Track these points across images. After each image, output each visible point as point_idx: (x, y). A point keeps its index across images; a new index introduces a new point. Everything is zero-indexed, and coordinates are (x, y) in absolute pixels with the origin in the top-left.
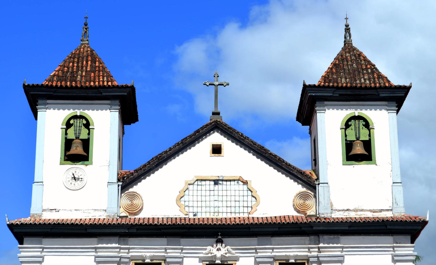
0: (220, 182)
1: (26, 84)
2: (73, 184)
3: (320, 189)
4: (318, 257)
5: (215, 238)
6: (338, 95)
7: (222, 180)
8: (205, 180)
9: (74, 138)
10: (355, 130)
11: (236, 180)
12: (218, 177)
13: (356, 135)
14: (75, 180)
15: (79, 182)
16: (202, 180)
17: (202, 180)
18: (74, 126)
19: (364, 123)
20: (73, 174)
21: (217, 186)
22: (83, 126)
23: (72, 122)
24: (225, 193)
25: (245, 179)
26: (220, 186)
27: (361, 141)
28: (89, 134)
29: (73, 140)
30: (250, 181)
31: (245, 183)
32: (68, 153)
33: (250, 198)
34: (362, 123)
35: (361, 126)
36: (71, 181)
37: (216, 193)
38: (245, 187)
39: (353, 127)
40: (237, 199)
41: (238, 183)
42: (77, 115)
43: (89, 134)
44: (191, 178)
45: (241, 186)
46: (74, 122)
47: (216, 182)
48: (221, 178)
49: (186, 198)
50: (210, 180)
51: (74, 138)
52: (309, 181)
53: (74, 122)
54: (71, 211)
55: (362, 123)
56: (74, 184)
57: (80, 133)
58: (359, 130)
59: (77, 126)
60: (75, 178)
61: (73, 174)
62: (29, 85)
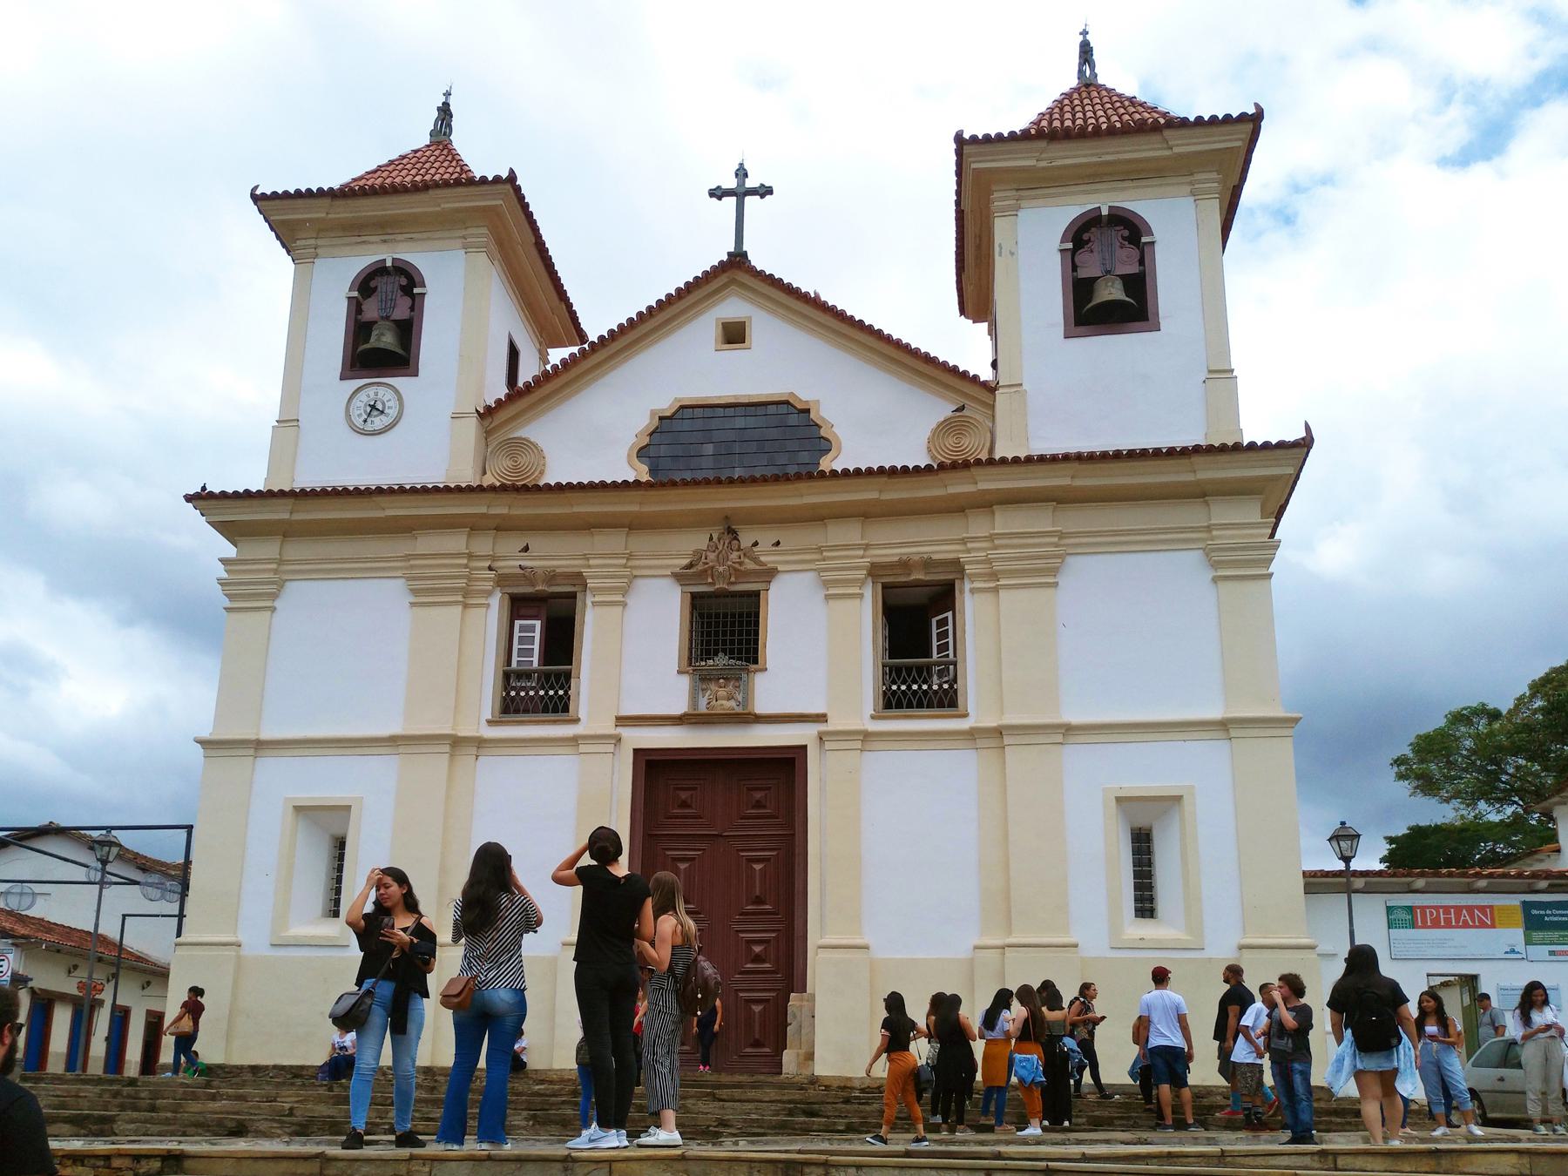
4: (988, 561)
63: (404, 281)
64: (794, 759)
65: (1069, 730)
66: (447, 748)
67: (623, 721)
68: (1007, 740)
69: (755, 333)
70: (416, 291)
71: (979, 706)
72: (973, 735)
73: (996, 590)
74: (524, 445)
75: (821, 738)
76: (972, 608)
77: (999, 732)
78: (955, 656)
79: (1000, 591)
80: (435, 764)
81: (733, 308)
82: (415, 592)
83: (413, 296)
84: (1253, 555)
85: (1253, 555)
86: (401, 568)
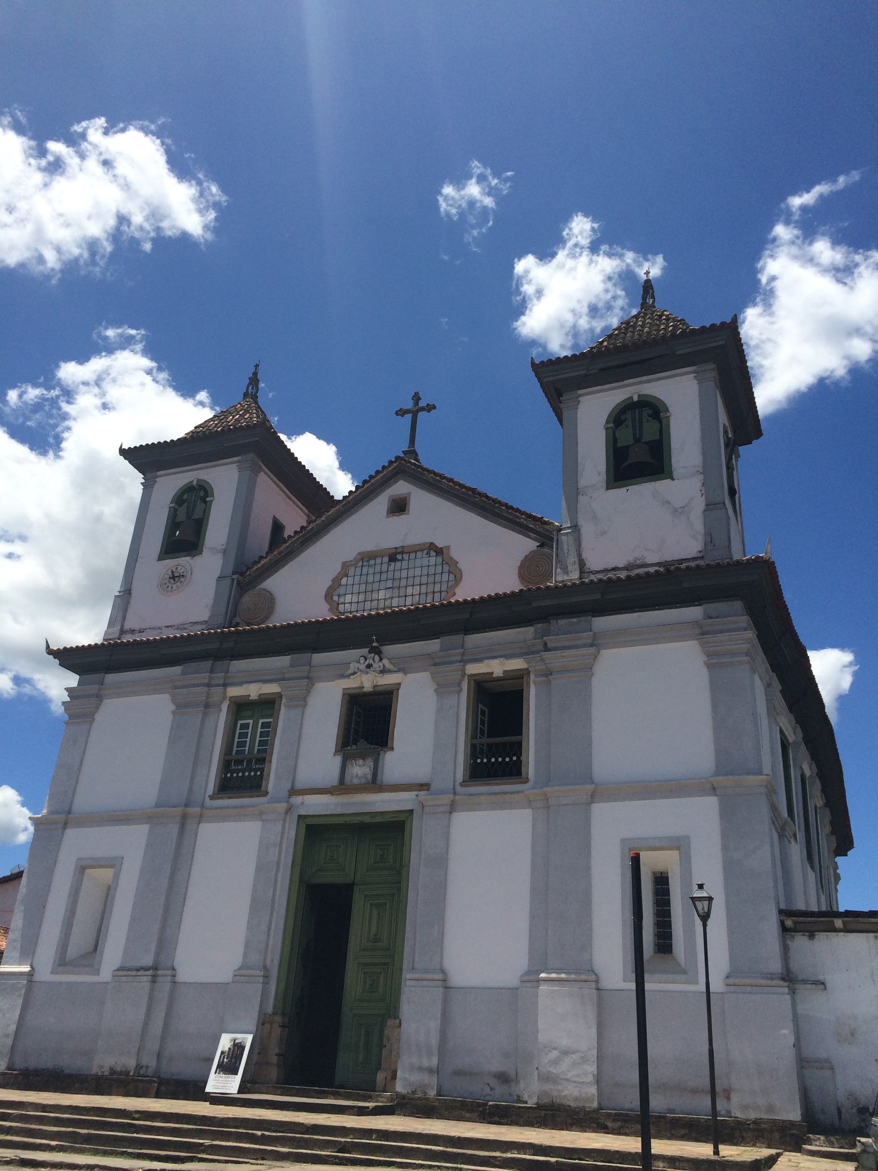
0: (399, 557)
2: (170, 588)
6: (596, 371)
7: (402, 553)
12: (396, 548)
13: (634, 435)
19: (650, 412)
21: (393, 564)
24: (404, 574)
25: (439, 545)
26: (398, 564)
27: (644, 443)
30: (448, 548)
31: (439, 552)
34: (647, 412)
37: (390, 575)
38: (439, 559)
40: (424, 580)
44: (350, 556)
47: (393, 556)
49: (342, 590)
52: (547, 530)
54: (160, 628)
55: (647, 412)
58: (641, 428)
61: (173, 572)
63: (202, 494)
69: (413, 504)
70: (208, 499)
81: (401, 487)
83: (205, 502)
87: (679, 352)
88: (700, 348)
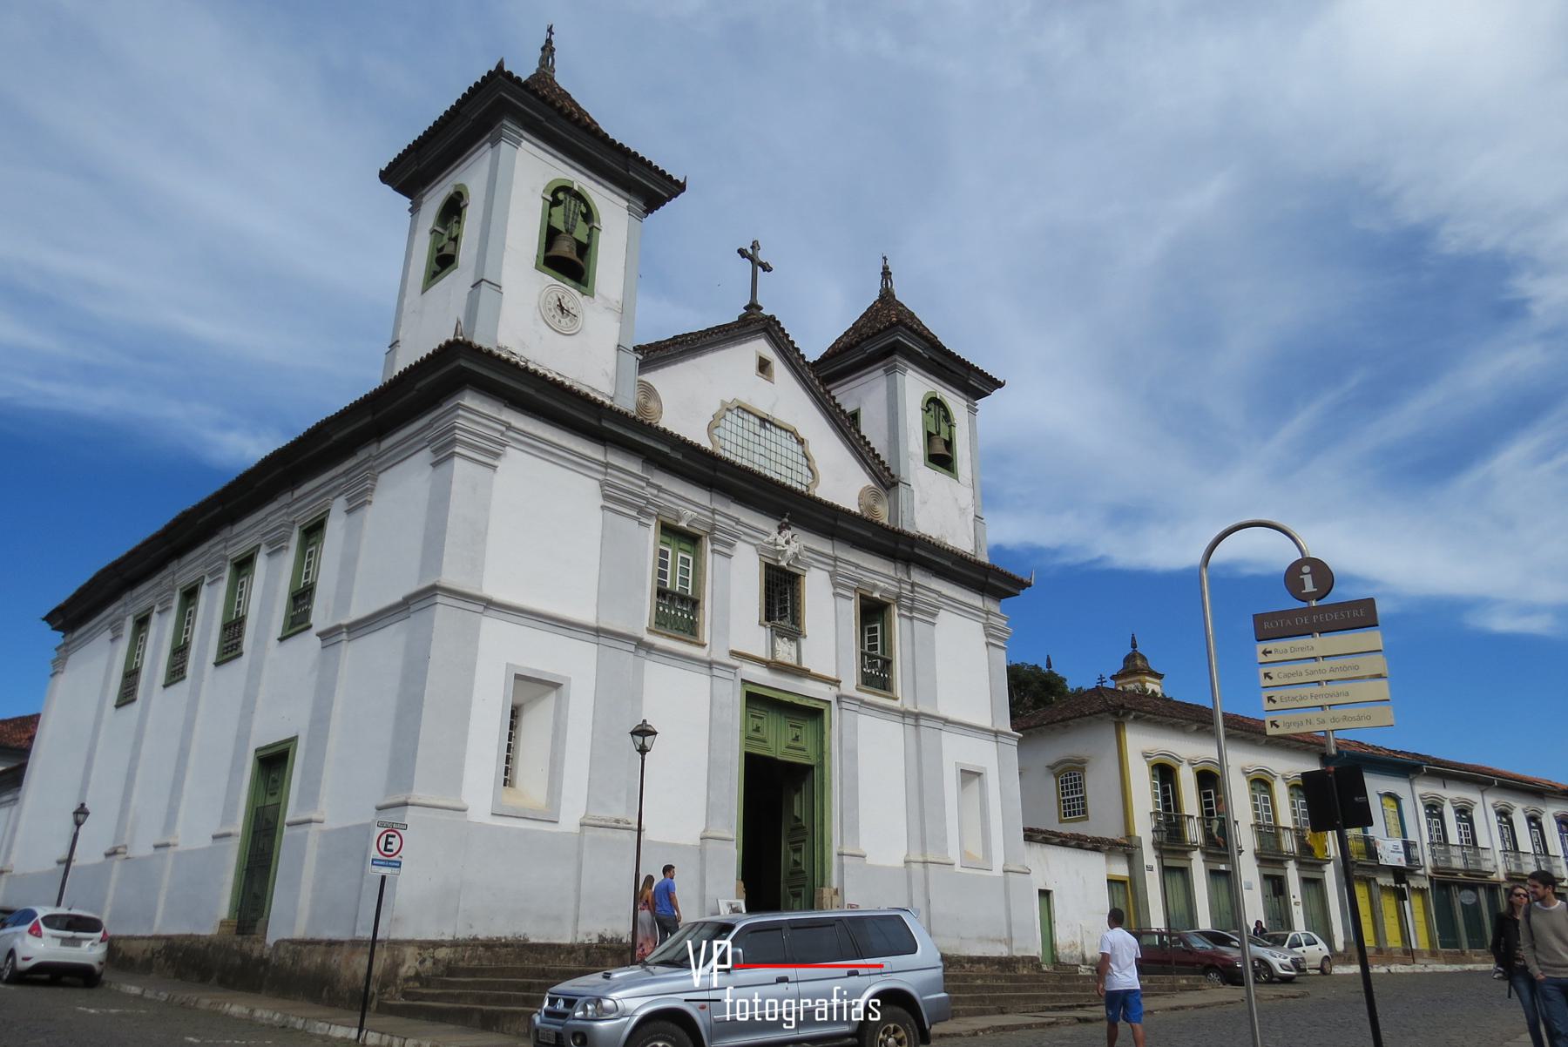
1: (506, 69)
3: (902, 488)
5: (777, 519)
8: (749, 412)
9: (564, 231)
10: (935, 419)
11: (790, 432)
14: (563, 313)
15: (567, 320)
16: (744, 410)
17: (744, 410)
18: (565, 207)
20: (559, 300)
22: (580, 216)
23: (561, 196)
25: (802, 434)
28: (589, 236)
29: (560, 232)
31: (801, 442)
32: (551, 253)
33: (805, 469)
35: (941, 418)
36: (554, 313)
39: (932, 413)
41: (790, 437)
42: (572, 189)
43: (589, 236)
45: (796, 447)
46: (566, 199)
47: (764, 421)
48: (770, 419)
49: (721, 432)
50: (755, 415)
51: (563, 229)
53: (566, 199)
56: (560, 321)
57: (574, 226)
59: (569, 210)
60: (562, 309)
61: (559, 300)
62: (510, 74)
64: (823, 710)
65: (946, 721)
66: (632, 648)
67: (734, 654)
68: (922, 722)
71: (903, 696)
72: (905, 714)
73: (911, 619)
74: (648, 391)
75: (839, 699)
76: (899, 625)
77: (917, 716)
78: (883, 652)
79: (915, 621)
80: (624, 656)
81: (761, 347)
82: (606, 497)
84: (931, 610)
85: (931, 610)
86: (597, 471)
87: (971, 382)
88: (980, 387)
